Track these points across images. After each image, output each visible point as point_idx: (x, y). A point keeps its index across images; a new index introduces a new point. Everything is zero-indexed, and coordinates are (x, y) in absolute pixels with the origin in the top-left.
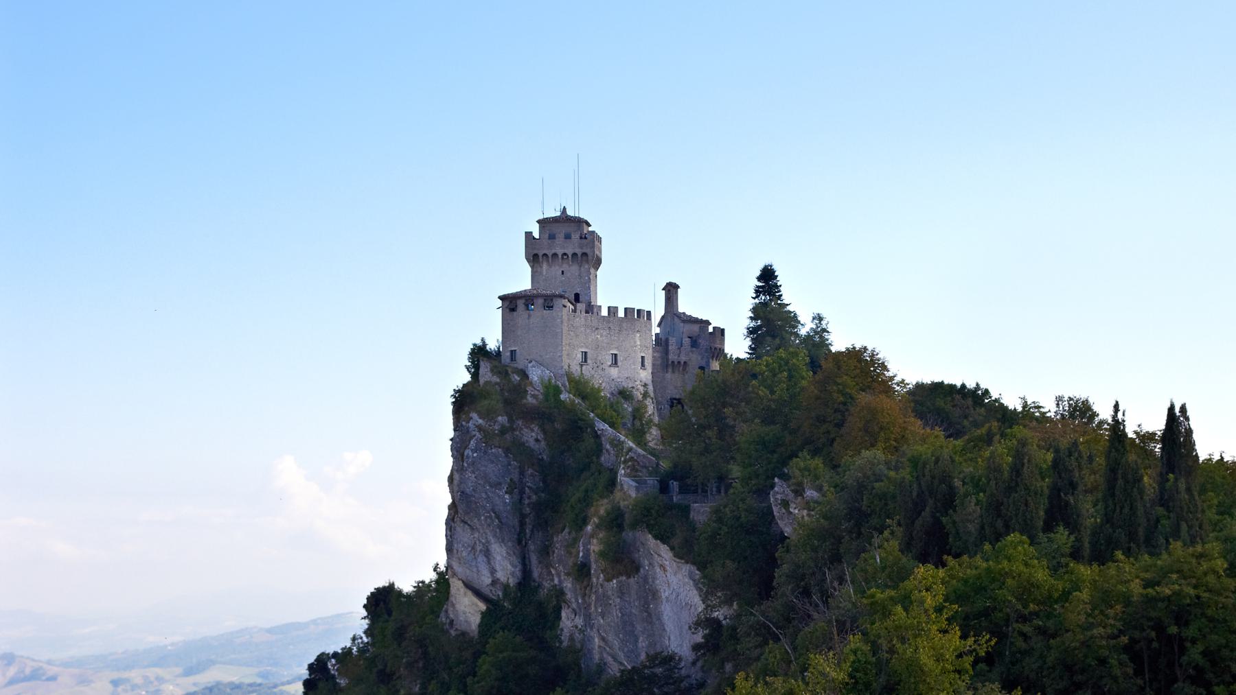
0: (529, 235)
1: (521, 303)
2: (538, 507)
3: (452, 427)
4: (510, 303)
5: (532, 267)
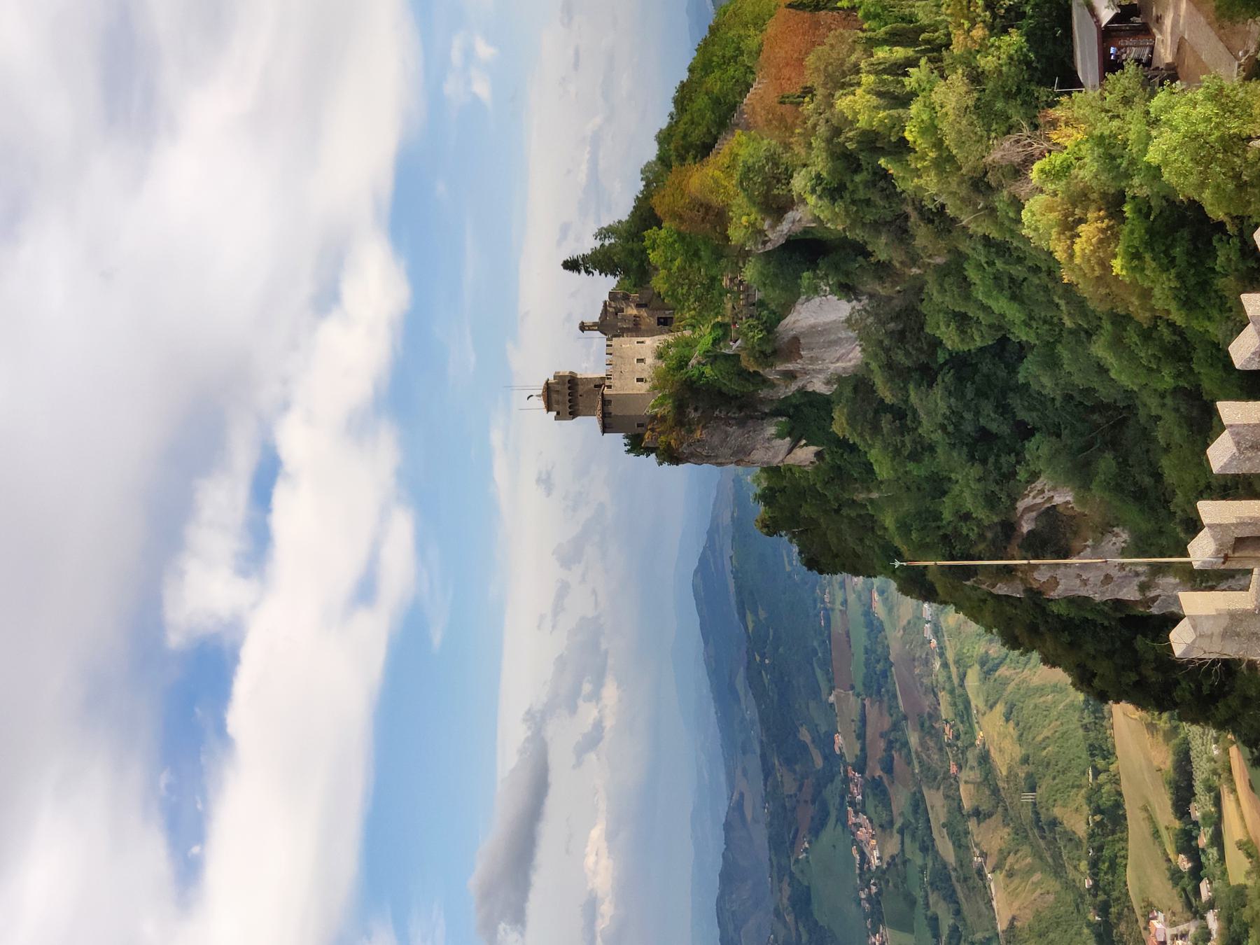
1: (608, 420)
2: (740, 408)
3: (688, 464)
4: (606, 428)
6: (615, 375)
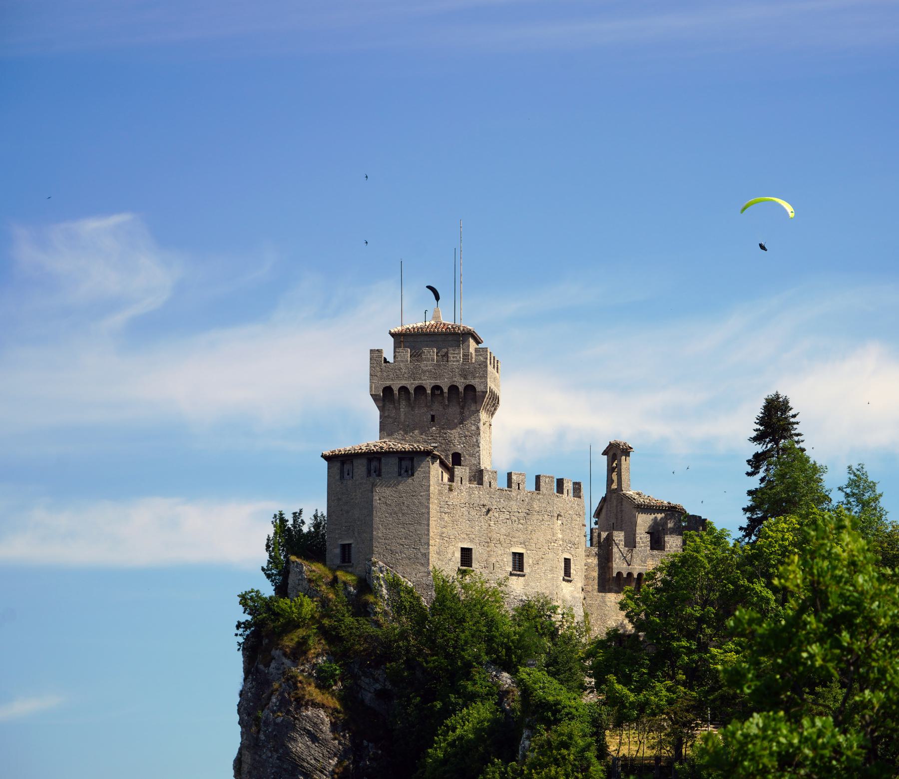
0: (376, 354)
1: (360, 468)
5: (382, 409)
6: (480, 494)
